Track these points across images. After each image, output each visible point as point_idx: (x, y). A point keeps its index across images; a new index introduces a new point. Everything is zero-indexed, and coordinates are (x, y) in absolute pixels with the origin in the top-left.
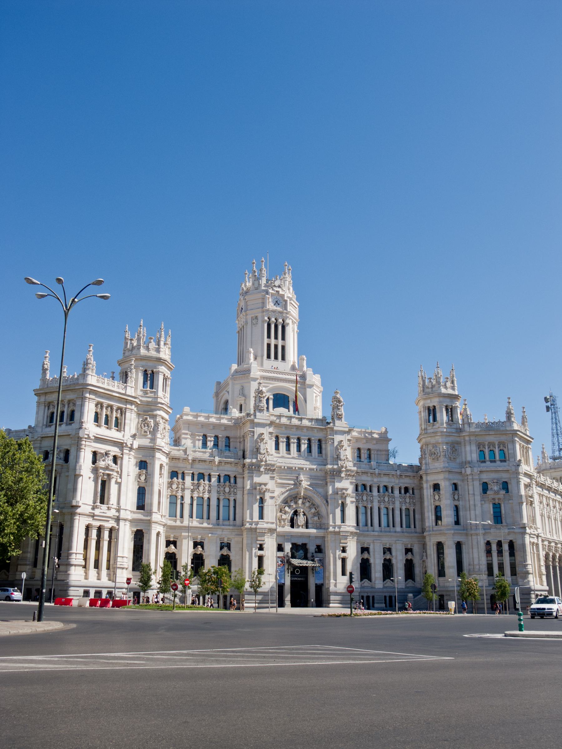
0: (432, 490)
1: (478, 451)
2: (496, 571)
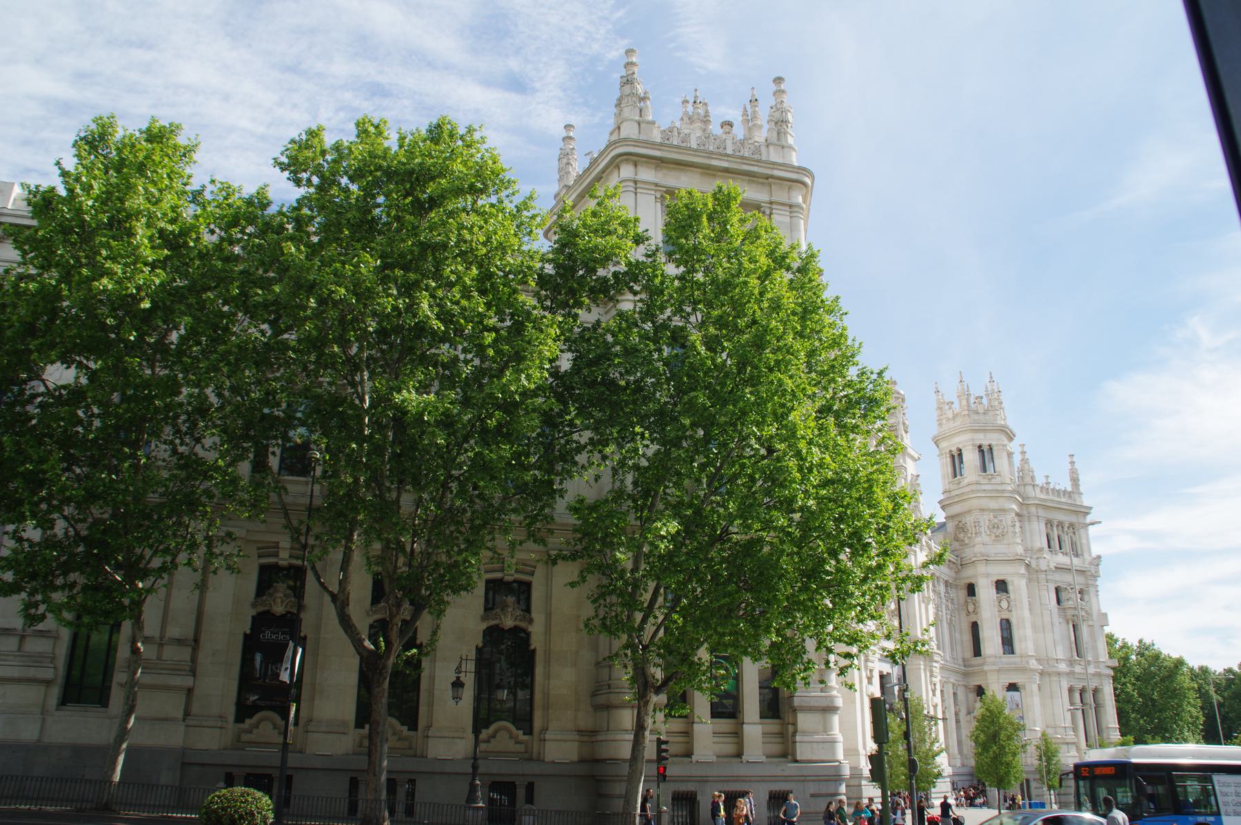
0: (995, 590)
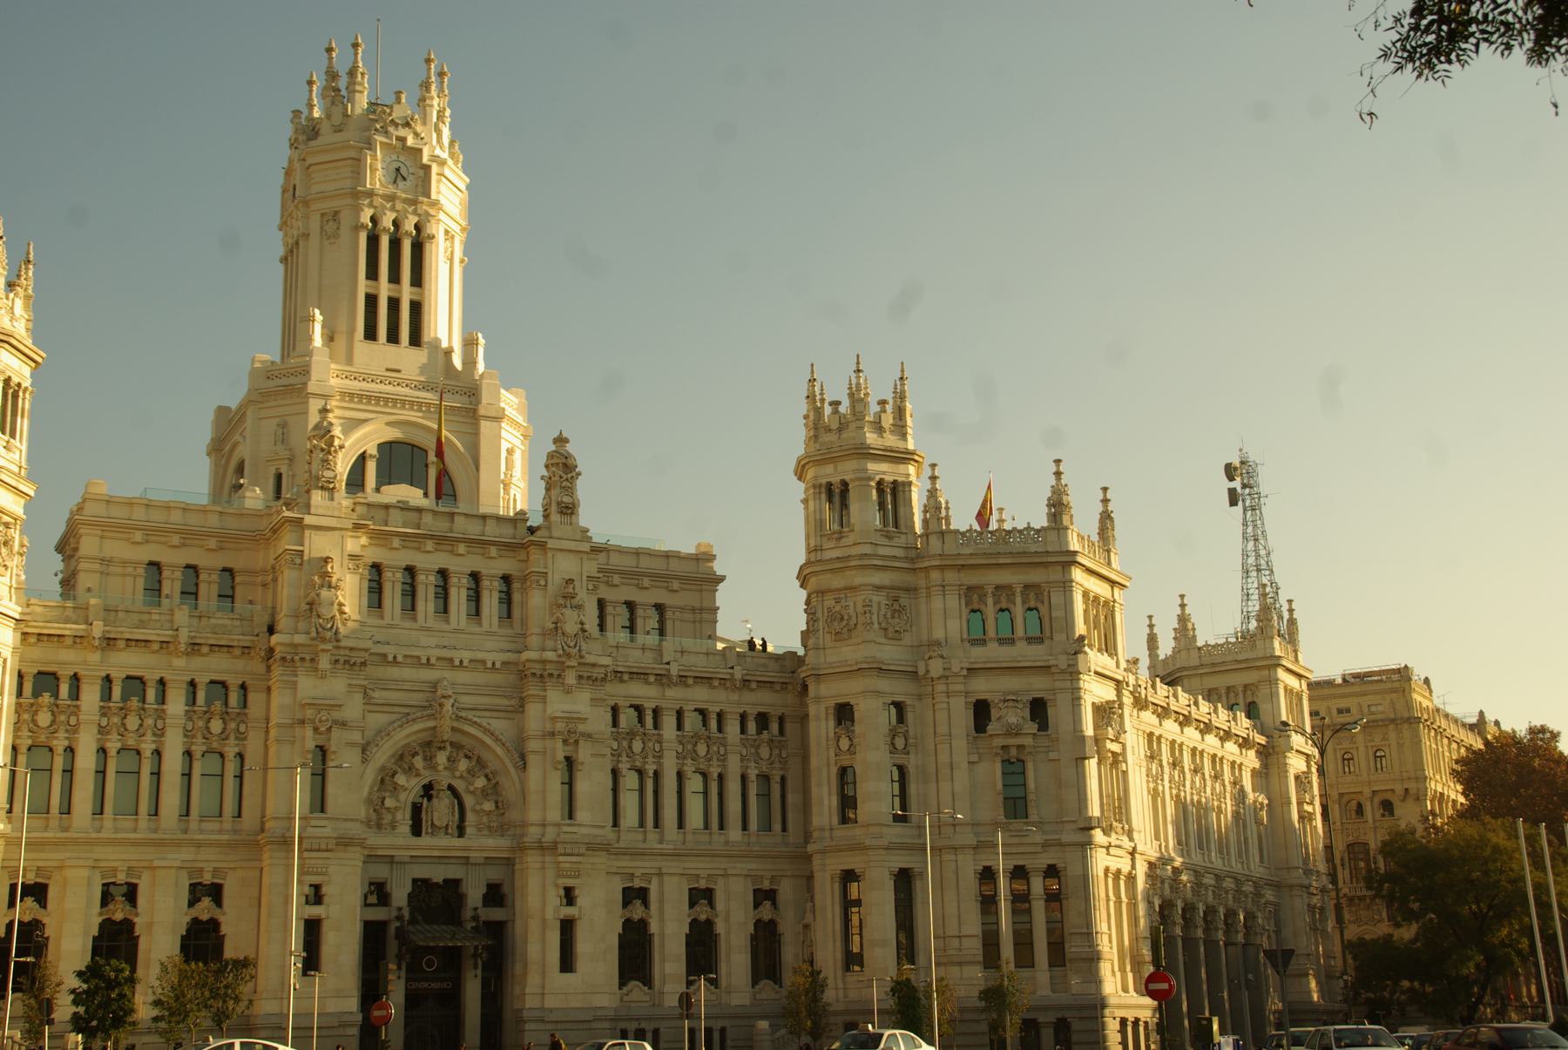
0: (832, 723)
1: (965, 611)
2: (1007, 950)
